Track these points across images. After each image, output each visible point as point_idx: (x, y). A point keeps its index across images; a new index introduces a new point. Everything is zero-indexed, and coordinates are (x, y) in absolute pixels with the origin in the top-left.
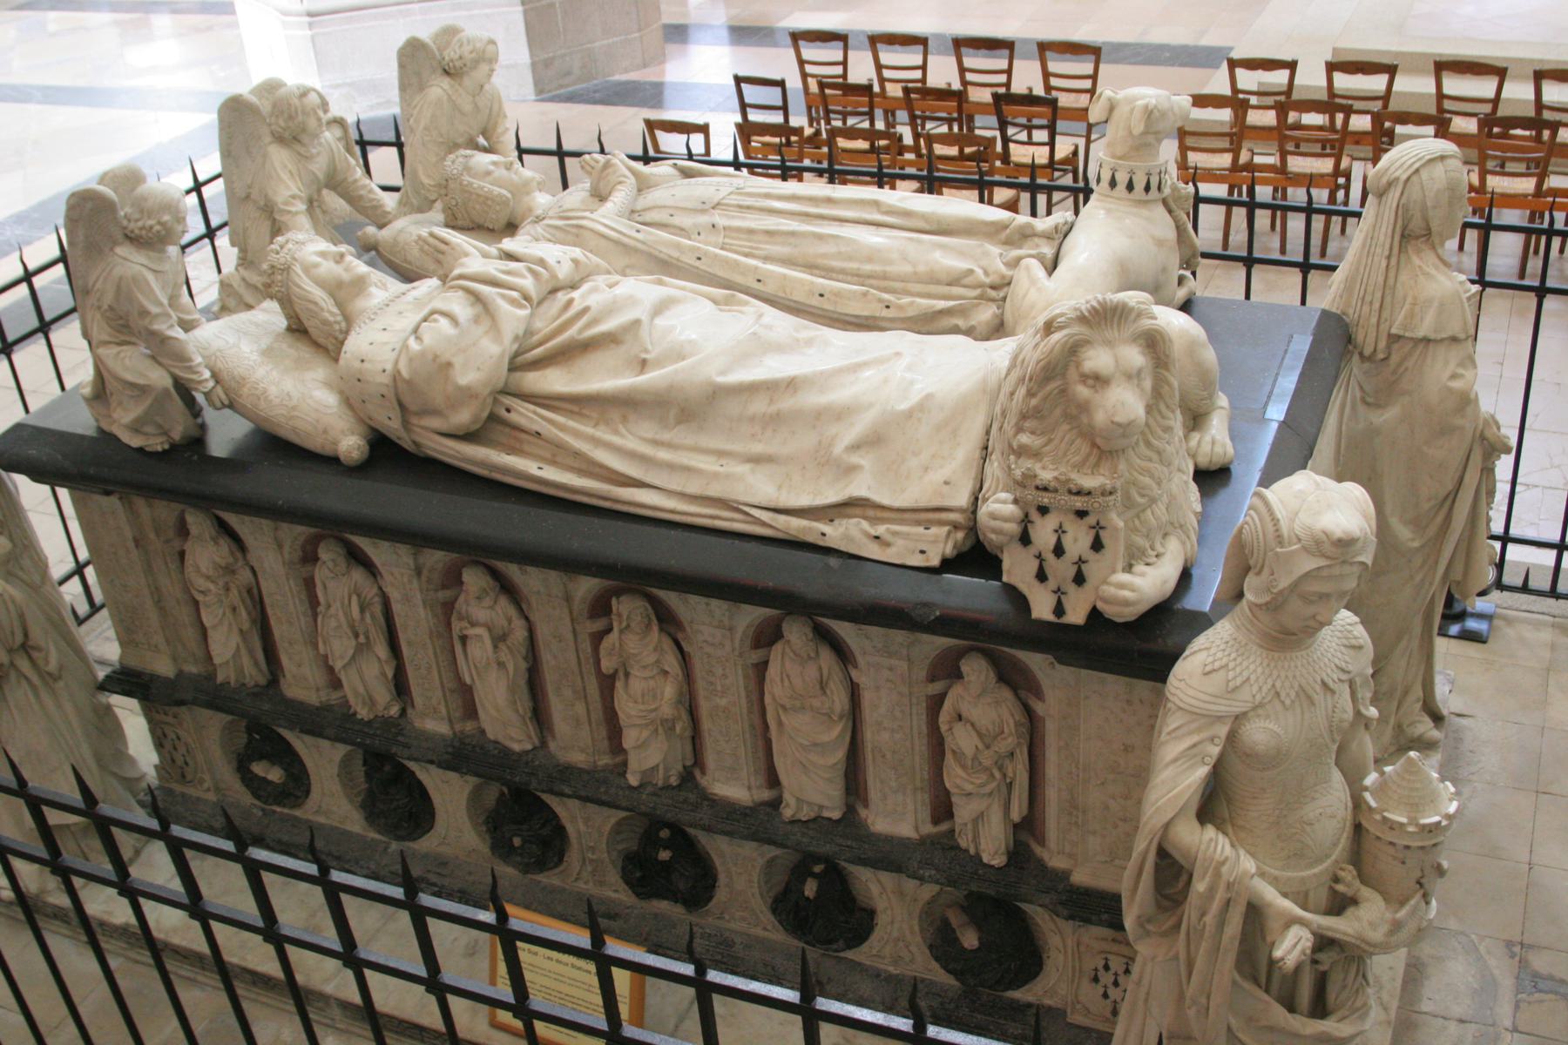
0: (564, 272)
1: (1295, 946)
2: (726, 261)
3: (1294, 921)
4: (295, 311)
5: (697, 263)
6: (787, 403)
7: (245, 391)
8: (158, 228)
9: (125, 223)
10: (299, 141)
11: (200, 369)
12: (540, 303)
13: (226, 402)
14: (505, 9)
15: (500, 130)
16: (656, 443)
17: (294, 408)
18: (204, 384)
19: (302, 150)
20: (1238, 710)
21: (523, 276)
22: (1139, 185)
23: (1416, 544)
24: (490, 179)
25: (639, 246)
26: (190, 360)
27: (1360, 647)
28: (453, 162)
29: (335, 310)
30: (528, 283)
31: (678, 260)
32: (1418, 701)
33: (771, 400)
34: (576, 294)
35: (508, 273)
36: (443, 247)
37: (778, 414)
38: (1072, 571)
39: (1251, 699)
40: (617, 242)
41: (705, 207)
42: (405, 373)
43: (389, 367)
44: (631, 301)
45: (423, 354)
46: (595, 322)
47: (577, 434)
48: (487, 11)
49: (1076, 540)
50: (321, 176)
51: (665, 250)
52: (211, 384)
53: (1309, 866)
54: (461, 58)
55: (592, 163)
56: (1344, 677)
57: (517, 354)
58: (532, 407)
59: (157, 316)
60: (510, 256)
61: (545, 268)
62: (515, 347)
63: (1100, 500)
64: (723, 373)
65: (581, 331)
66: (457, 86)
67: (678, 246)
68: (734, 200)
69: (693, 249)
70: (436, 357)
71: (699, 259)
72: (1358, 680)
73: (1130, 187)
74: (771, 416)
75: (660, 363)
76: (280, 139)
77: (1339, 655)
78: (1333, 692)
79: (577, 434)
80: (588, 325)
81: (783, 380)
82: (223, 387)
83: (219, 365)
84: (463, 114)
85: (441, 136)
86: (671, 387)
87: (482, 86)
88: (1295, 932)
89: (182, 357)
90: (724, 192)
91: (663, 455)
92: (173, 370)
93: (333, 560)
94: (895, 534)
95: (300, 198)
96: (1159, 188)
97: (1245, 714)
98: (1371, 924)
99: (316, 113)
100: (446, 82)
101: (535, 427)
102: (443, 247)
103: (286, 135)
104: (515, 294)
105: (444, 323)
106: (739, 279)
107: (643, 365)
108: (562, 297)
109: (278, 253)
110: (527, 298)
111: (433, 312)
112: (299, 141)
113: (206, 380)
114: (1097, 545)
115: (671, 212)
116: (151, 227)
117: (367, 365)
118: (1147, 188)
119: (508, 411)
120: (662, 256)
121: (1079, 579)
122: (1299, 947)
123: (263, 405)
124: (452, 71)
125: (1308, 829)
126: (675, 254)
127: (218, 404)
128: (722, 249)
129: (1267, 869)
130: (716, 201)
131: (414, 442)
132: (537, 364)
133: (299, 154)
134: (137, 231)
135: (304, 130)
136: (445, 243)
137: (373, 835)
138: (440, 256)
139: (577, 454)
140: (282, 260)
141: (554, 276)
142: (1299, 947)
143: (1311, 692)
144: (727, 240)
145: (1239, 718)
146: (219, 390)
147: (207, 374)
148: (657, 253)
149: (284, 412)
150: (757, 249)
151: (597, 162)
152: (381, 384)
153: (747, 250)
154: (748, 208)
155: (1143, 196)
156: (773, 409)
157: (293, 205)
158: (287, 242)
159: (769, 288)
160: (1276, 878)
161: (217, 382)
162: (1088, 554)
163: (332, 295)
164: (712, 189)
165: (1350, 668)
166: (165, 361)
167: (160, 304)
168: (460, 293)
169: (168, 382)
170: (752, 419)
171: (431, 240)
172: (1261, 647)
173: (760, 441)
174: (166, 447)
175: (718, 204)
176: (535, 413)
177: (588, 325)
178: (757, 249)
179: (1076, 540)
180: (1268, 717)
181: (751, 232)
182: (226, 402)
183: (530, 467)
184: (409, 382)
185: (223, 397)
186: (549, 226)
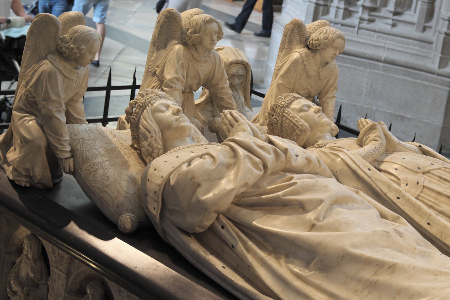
0: (298, 162)
2: (414, 205)
4: (138, 135)
5: (396, 201)
6: (383, 278)
7: (85, 166)
8: (76, 50)
9: (60, 42)
10: (196, 49)
11: (65, 144)
12: (273, 174)
13: (72, 170)
14: (438, 86)
15: (329, 95)
16: (298, 276)
17: (107, 186)
18: (64, 154)
19: (196, 55)
21: (269, 153)
24: (302, 114)
25: (366, 177)
26: (62, 136)
28: (285, 97)
29: (160, 141)
30: (270, 158)
31: (385, 194)
33: (376, 273)
34: (296, 176)
35: (261, 147)
36: (233, 121)
37: (376, 283)
40: (354, 172)
41: (419, 171)
42: (172, 182)
43: (165, 175)
44: (325, 188)
45: (187, 173)
46: (297, 193)
47: (255, 255)
48: (426, 83)
50: (202, 76)
51: (380, 186)
52: (68, 155)
54: (318, 40)
55: (364, 123)
57: (243, 195)
58: (237, 230)
59: (54, 101)
60: (271, 142)
61: (286, 156)
62: (243, 190)
64: (355, 247)
65: (285, 195)
66: (311, 57)
67: (389, 186)
68: (437, 173)
69: (397, 191)
70: (193, 177)
71: (398, 198)
74: (371, 282)
75: (321, 229)
76: (185, 44)
79: (255, 255)
80: (291, 193)
81: (388, 263)
82: (74, 160)
83: (78, 146)
84: (308, 76)
85: (290, 83)
86: (320, 244)
87: (327, 63)
89: (57, 133)
90: (436, 166)
91: (298, 284)
92: (49, 137)
93: (93, 295)
95: (182, 82)
99: (212, 36)
100: (304, 50)
101: (233, 242)
102: (233, 121)
103: (189, 42)
104: (258, 160)
105: (208, 159)
106: (417, 218)
107: (313, 227)
108: (289, 175)
109: (143, 96)
110: (265, 167)
111: (207, 154)
112: (196, 49)
113: (66, 151)
115: (396, 166)
116: (73, 49)
117: (156, 172)
119: (223, 227)
120: (377, 189)
123: (91, 178)
124: (310, 47)
126: (385, 190)
127: (67, 170)
128: (417, 198)
130: (427, 169)
131: (163, 230)
132: (252, 206)
133: (193, 56)
134: (64, 49)
135: (201, 43)
136: (237, 121)
138: (230, 127)
139: (250, 267)
140: (143, 101)
141: (288, 161)
144: (421, 194)
146: (71, 161)
147: (68, 149)
148: (374, 186)
149: (101, 187)
150: (437, 205)
151: (367, 123)
152: (157, 184)
153: (430, 204)
154: (445, 180)
156: (375, 278)
157: (175, 84)
158: (152, 92)
159: (433, 230)
161: (72, 156)
163: (162, 131)
164: (429, 163)
166: (48, 131)
167: (58, 95)
168: (228, 147)
169: (43, 143)
170: (360, 281)
171: (229, 116)
173: (358, 296)
174: (28, 185)
175: (428, 172)
176: (237, 234)
177: (291, 193)
178: (437, 205)
181: (439, 193)
182: (72, 170)
183: (218, 264)
184: (173, 187)
185: (72, 166)
186: (321, 151)
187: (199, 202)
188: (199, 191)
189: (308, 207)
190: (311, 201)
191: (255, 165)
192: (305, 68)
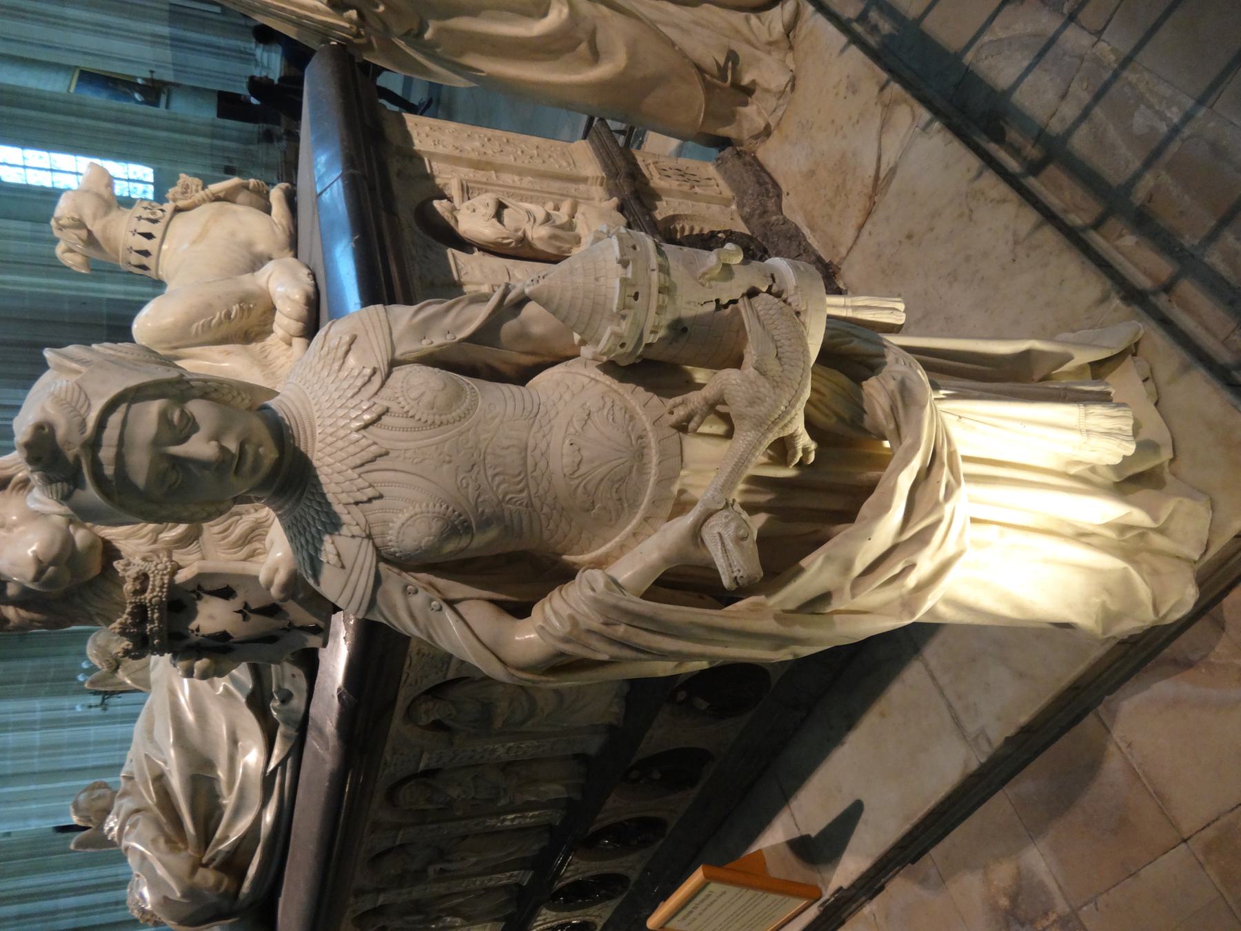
1: (725, 550)
3: (696, 534)
20: (367, 557)
22: (145, 244)
23: (566, 10)
27: (353, 340)
32: (747, 20)
38: (256, 620)
39: (359, 540)
49: (211, 617)
53: (642, 470)
56: (377, 380)
63: (148, 595)
72: (405, 348)
73: (146, 253)
77: (345, 384)
78: (387, 411)
88: (710, 533)
94: (280, 689)
96: (154, 221)
97: (376, 548)
98: (751, 403)
110: (137, 811)
114: (226, 593)
118: (149, 236)
121: (271, 610)
122: (730, 545)
125: (583, 469)
129: (629, 528)
137: (624, 896)
142: (730, 545)
143: (366, 455)
145: (382, 556)
155: (155, 242)
160: (646, 519)
162: (236, 603)
165: (368, 371)
172: (298, 500)
179: (211, 617)
180: (385, 523)
187: (184, 895)
188: (172, 897)
189: (158, 772)
190: (150, 768)
191: (133, 826)
192: (140, 669)
